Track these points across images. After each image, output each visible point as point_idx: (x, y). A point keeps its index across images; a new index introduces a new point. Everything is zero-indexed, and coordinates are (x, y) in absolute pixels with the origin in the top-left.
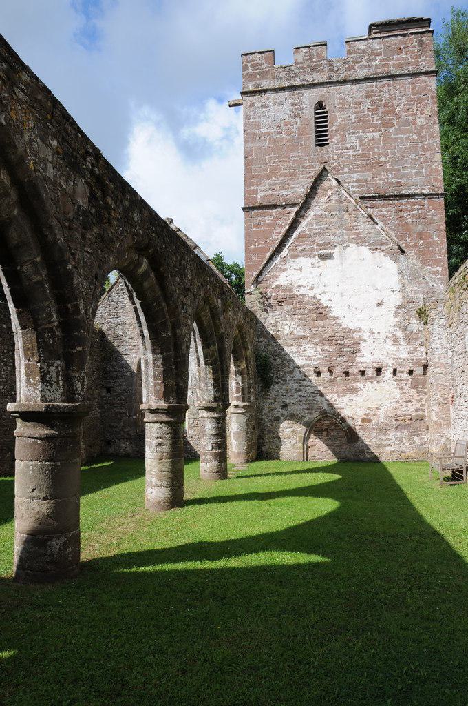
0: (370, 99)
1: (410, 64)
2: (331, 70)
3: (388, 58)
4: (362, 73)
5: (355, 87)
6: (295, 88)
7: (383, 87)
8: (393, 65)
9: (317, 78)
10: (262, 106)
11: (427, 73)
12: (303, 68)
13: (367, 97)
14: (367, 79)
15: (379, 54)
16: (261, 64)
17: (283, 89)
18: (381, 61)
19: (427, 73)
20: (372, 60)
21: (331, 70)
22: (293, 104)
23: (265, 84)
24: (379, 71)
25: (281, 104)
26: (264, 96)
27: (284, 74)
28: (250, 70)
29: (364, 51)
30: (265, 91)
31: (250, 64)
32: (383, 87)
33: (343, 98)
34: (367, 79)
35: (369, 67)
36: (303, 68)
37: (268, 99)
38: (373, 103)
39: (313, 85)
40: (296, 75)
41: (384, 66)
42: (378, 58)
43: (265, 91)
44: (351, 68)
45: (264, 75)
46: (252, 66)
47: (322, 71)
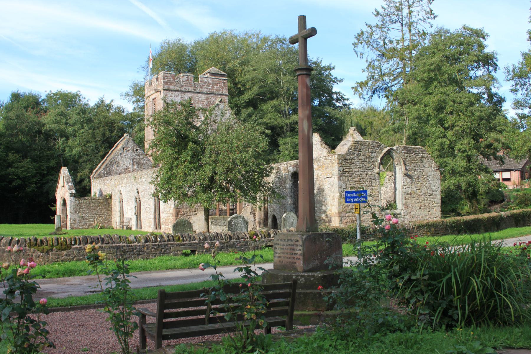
0: (207, 101)
1: (220, 90)
2: (195, 87)
3: (213, 87)
4: (205, 90)
5: (203, 95)
6: (182, 91)
7: (211, 97)
8: (215, 89)
9: (190, 89)
10: (170, 96)
11: (226, 95)
12: (185, 84)
13: (206, 100)
14: (207, 93)
15: (211, 84)
16: (170, 79)
17: (178, 91)
18: (211, 87)
19: (226, 95)
20: (208, 86)
21: (195, 87)
22: (181, 98)
23: (172, 87)
24: (210, 91)
25: (177, 96)
26: (171, 93)
27: (178, 85)
28: (166, 80)
29: (206, 82)
30: (171, 90)
31: (166, 78)
32: (211, 97)
33: (198, 99)
34: (207, 93)
35: (207, 88)
36: (185, 84)
37: (172, 93)
38: (208, 102)
39: (189, 92)
40: (183, 86)
41: (212, 89)
42: (210, 86)
43: (171, 90)
44: (201, 88)
45: (171, 83)
46: (167, 78)
47: (191, 86)
